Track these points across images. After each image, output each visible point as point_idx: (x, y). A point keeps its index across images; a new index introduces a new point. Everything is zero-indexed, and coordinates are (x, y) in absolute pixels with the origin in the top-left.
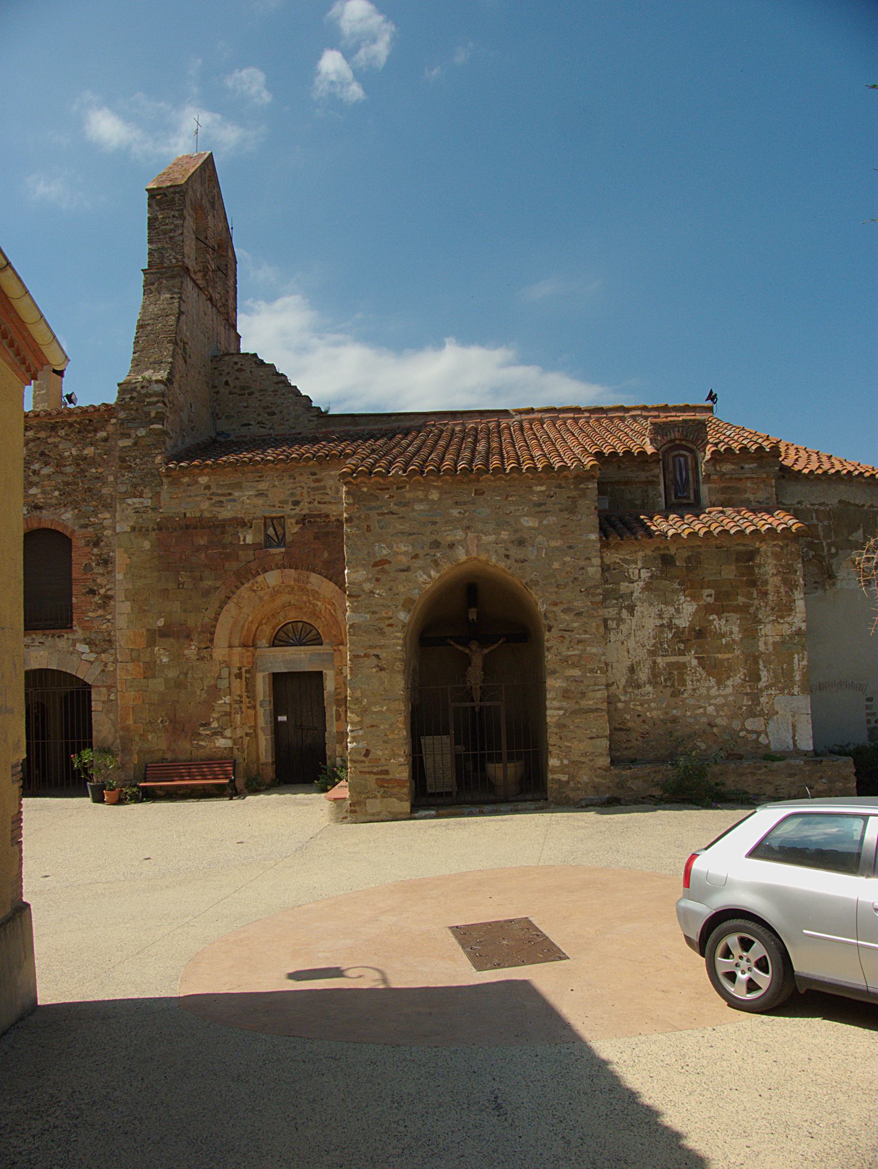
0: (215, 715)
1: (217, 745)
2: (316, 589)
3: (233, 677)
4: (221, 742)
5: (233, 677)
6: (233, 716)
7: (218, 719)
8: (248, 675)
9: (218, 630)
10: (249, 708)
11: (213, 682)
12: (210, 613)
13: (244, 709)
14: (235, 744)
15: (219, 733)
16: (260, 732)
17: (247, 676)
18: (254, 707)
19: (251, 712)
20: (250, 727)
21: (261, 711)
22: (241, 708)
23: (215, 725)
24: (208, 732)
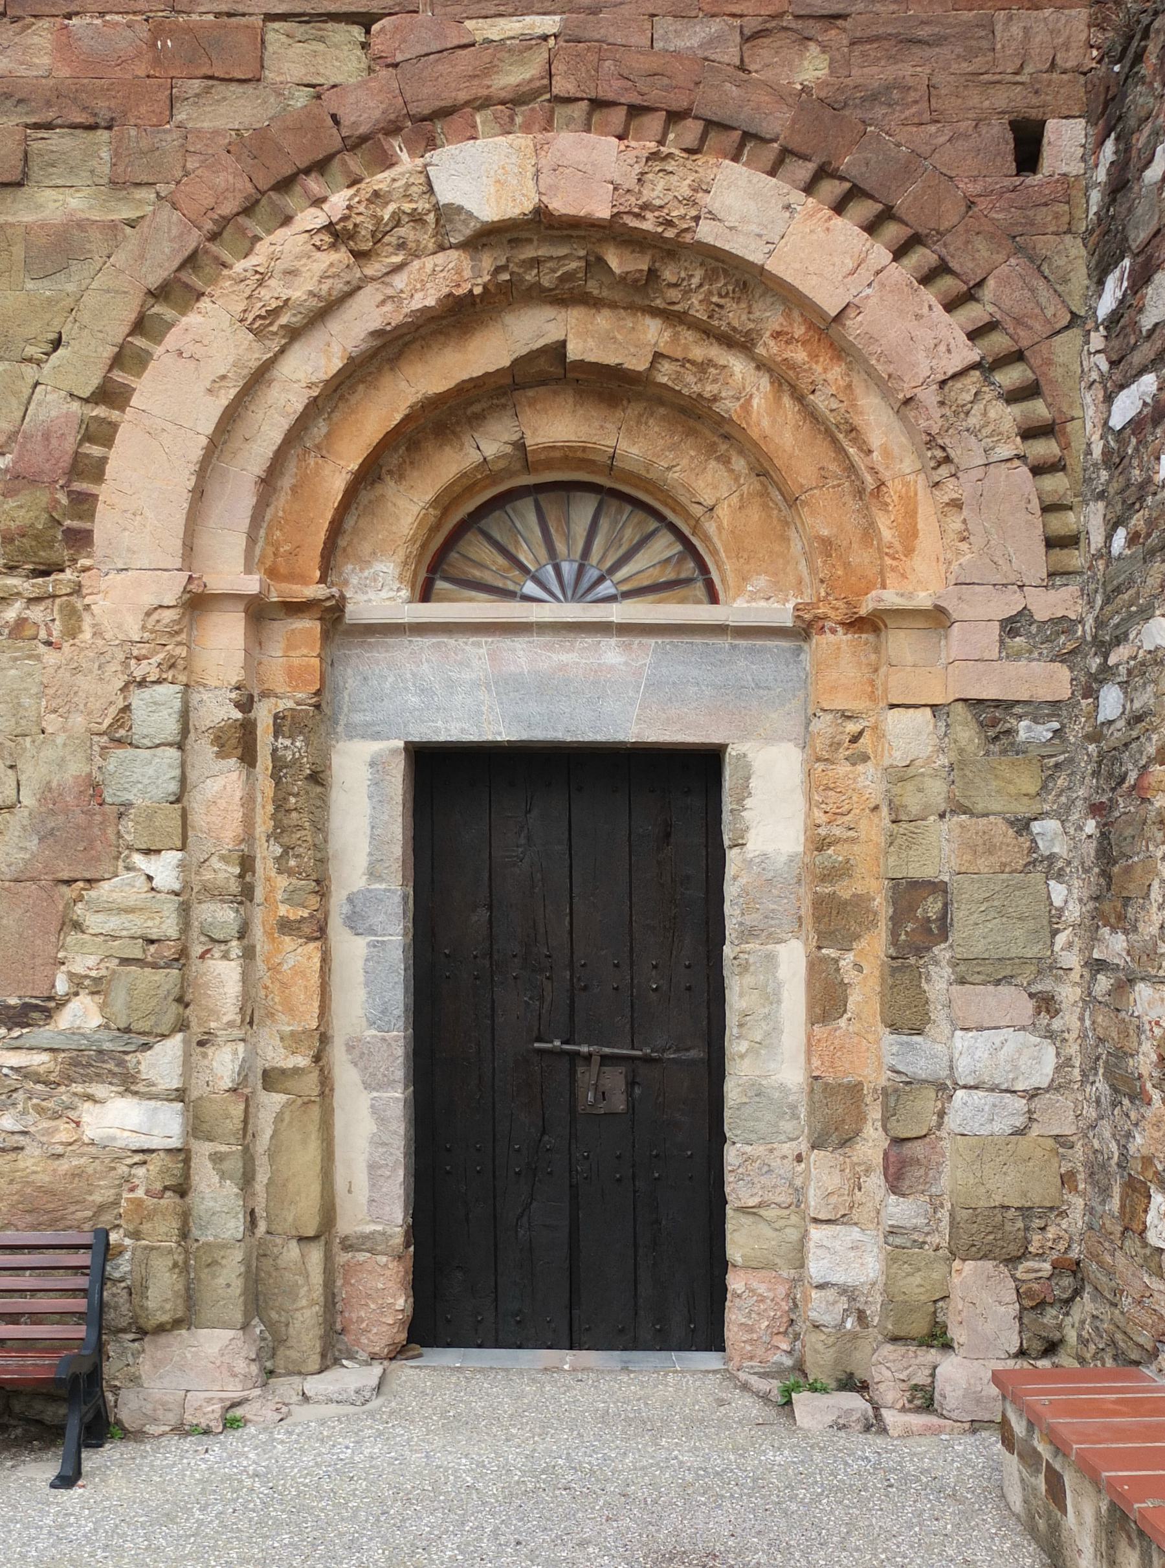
0: (84, 963)
1: (90, 1132)
2: (754, 254)
3: (203, 749)
4: (119, 1120)
5: (203, 749)
6: (196, 966)
7: (98, 987)
8: (294, 747)
9: (125, 461)
10: (286, 926)
11: (76, 768)
12: (82, 363)
13: (258, 933)
14: (197, 1127)
15: (104, 1064)
16: (346, 1075)
17: (288, 759)
18: (319, 932)
19: (299, 956)
20: (293, 1041)
21: (351, 950)
22: (243, 933)
23: (81, 1016)
24: (38, 1060)
